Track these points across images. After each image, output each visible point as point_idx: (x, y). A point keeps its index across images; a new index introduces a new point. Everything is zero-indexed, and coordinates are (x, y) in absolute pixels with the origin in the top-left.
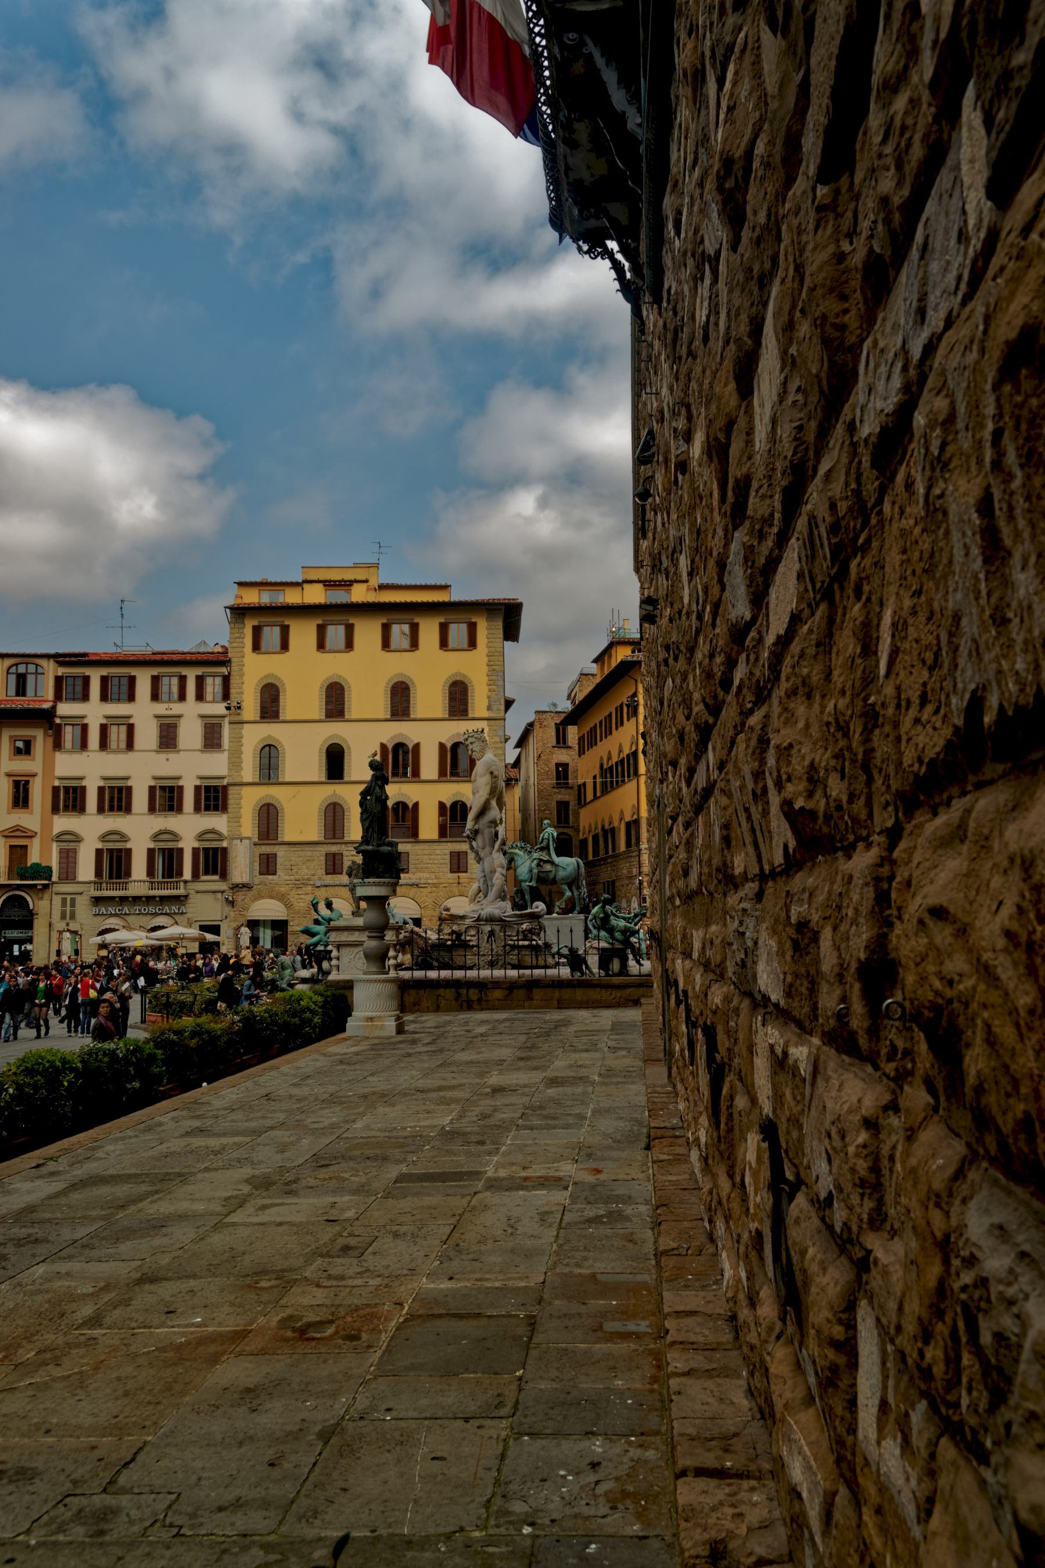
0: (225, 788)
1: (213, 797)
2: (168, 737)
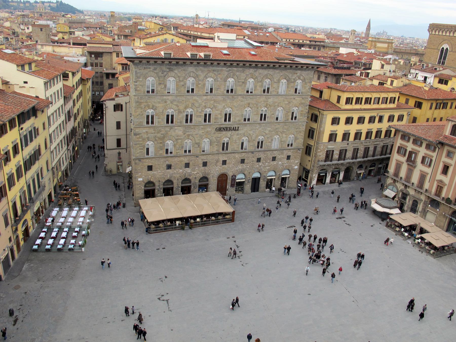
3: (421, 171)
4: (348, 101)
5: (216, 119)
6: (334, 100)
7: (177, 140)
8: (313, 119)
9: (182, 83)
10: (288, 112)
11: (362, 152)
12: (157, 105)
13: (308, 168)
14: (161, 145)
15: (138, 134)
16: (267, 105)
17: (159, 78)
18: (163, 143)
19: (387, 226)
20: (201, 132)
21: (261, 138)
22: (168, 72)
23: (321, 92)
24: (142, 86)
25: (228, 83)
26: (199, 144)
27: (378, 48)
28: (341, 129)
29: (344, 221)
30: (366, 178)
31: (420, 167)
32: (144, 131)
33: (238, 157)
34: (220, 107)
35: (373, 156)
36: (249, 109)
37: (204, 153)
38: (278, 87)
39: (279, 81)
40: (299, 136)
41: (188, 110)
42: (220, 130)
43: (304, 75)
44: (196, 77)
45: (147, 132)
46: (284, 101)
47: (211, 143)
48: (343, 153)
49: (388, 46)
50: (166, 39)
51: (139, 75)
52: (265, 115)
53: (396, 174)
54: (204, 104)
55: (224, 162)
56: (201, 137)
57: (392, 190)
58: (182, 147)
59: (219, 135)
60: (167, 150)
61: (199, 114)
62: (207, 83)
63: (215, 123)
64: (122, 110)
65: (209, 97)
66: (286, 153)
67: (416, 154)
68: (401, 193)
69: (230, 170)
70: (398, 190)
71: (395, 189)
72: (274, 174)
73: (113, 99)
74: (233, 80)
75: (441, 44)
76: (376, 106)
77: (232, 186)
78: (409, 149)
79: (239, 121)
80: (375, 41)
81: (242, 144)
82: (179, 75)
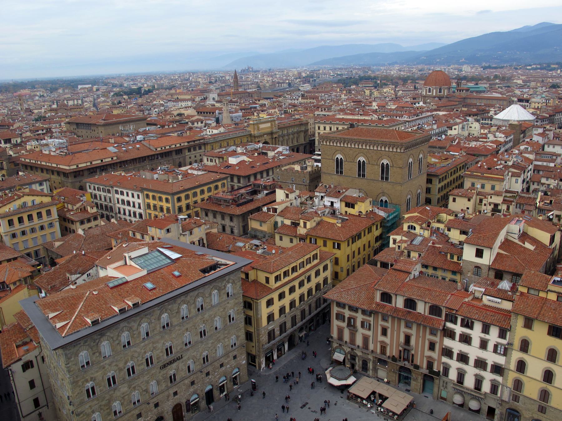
0: (504, 369)
1: (497, 369)
2: (484, 345)
3: (363, 334)
4: (277, 279)
5: (158, 359)
6: (263, 281)
7: (123, 398)
8: (247, 306)
9: (117, 342)
10: (225, 318)
11: (300, 317)
12: (96, 375)
13: (254, 353)
14: (109, 411)
15: (82, 413)
16: (204, 321)
17: (92, 349)
18: (110, 408)
19: (348, 398)
20: (146, 378)
21: (205, 354)
22: (101, 338)
23: (247, 275)
24: (76, 364)
25: (162, 320)
26: (146, 391)
27: (262, 129)
28: (275, 308)
29: (309, 408)
30: (308, 336)
31: (361, 332)
32: (87, 406)
33: (187, 382)
34: (159, 345)
35: (310, 314)
36: (188, 333)
37: (154, 396)
38: (211, 300)
39: (210, 294)
40: (240, 334)
41: (129, 364)
42: (164, 366)
43: (232, 278)
44: (130, 329)
45: (90, 406)
46: (219, 310)
47: (158, 383)
48: (283, 328)
49: (272, 125)
50: (25, 203)
51: (69, 355)
52: (204, 331)
53: (340, 338)
54: (143, 351)
55: (175, 394)
56: (148, 382)
57: (340, 353)
58: (131, 402)
59: (165, 372)
60: (115, 413)
61: (140, 363)
62: (142, 330)
63: (158, 362)
64: (33, 367)
65: (146, 342)
66: (231, 355)
67: (355, 320)
68: (349, 355)
69: (182, 399)
70: (345, 352)
71: (342, 351)
72: (224, 378)
73: (20, 359)
74: (166, 314)
75: (334, 154)
76: (302, 270)
77: (188, 411)
78: (347, 316)
79: (181, 349)
80: (257, 124)
81: (189, 367)
82: (112, 335)
